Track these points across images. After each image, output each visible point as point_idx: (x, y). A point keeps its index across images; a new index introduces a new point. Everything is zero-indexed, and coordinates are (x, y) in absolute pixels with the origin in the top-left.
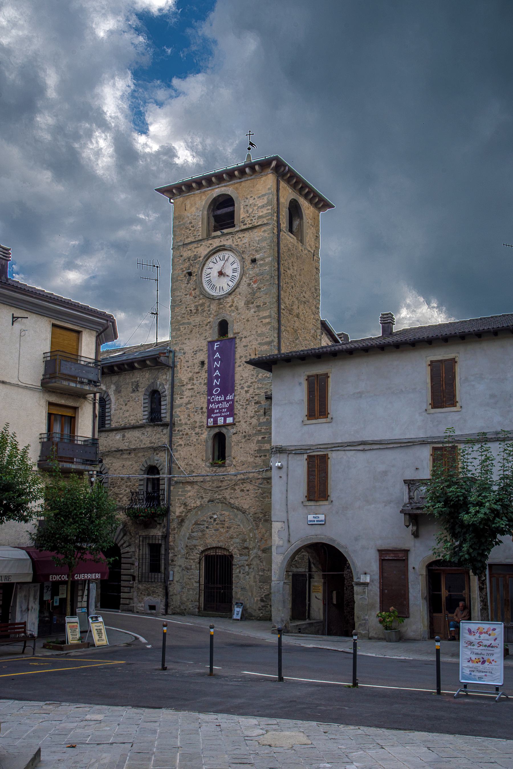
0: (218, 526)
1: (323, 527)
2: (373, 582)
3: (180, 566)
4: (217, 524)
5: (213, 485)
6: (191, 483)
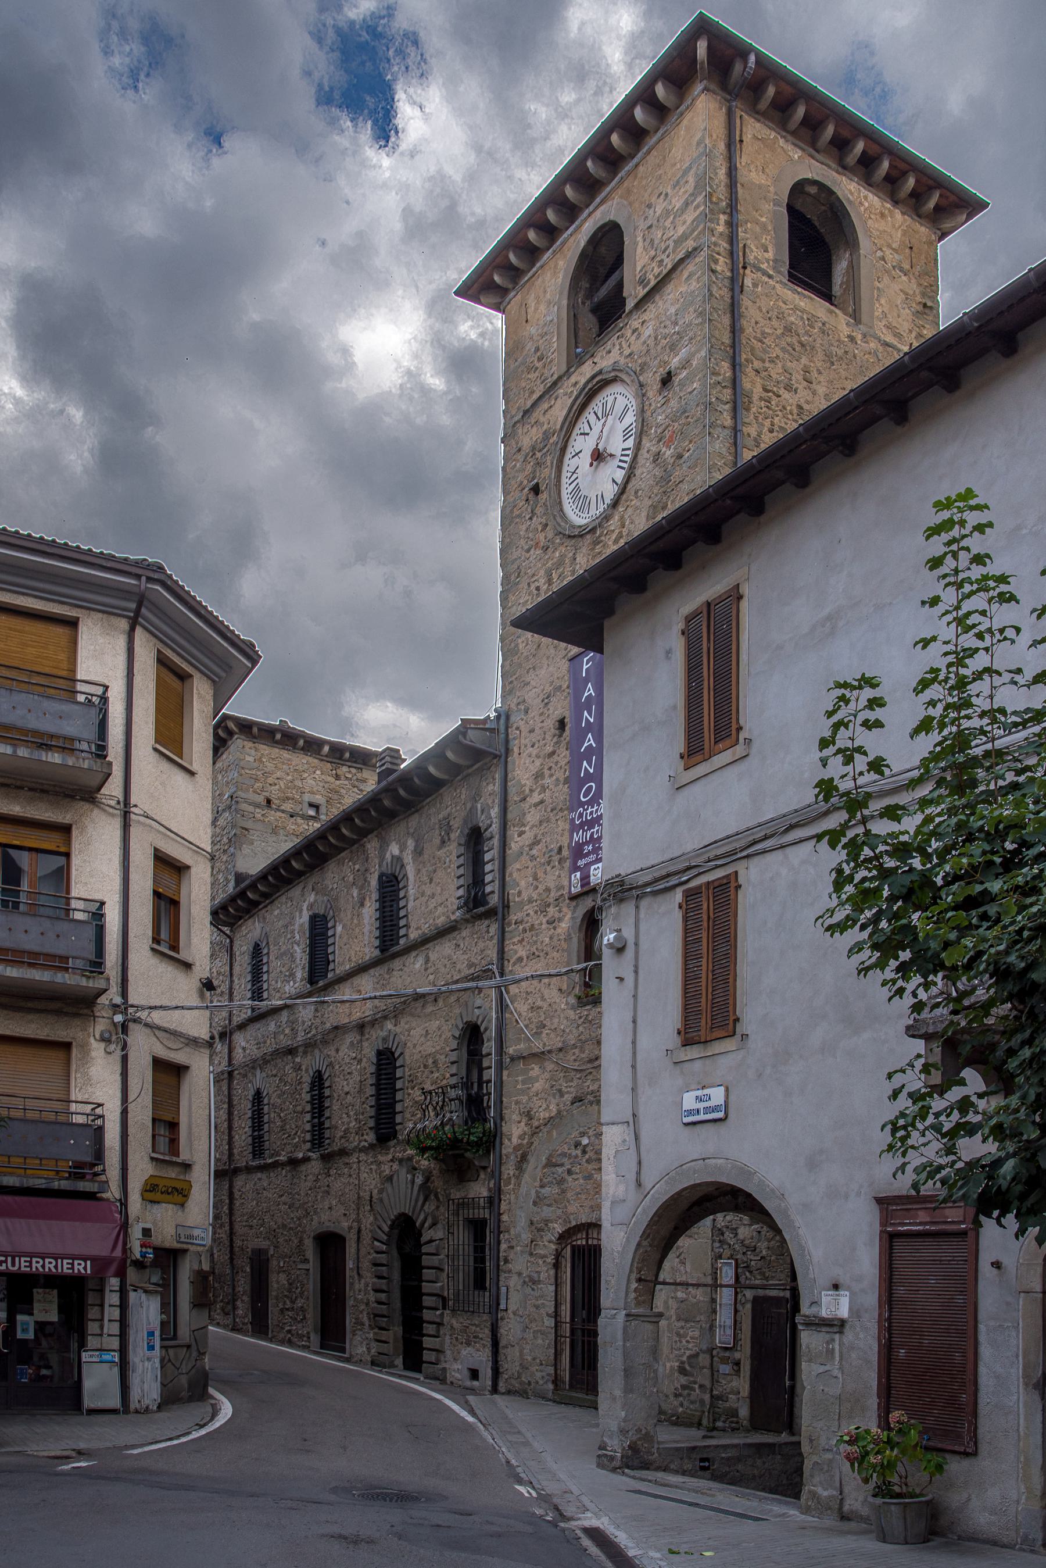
0: (590, 1167)
1: (722, 1128)
2: (859, 1317)
3: (520, 1274)
4: (588, 1161)
5: (583, 1056)
6: (539, 1056)
